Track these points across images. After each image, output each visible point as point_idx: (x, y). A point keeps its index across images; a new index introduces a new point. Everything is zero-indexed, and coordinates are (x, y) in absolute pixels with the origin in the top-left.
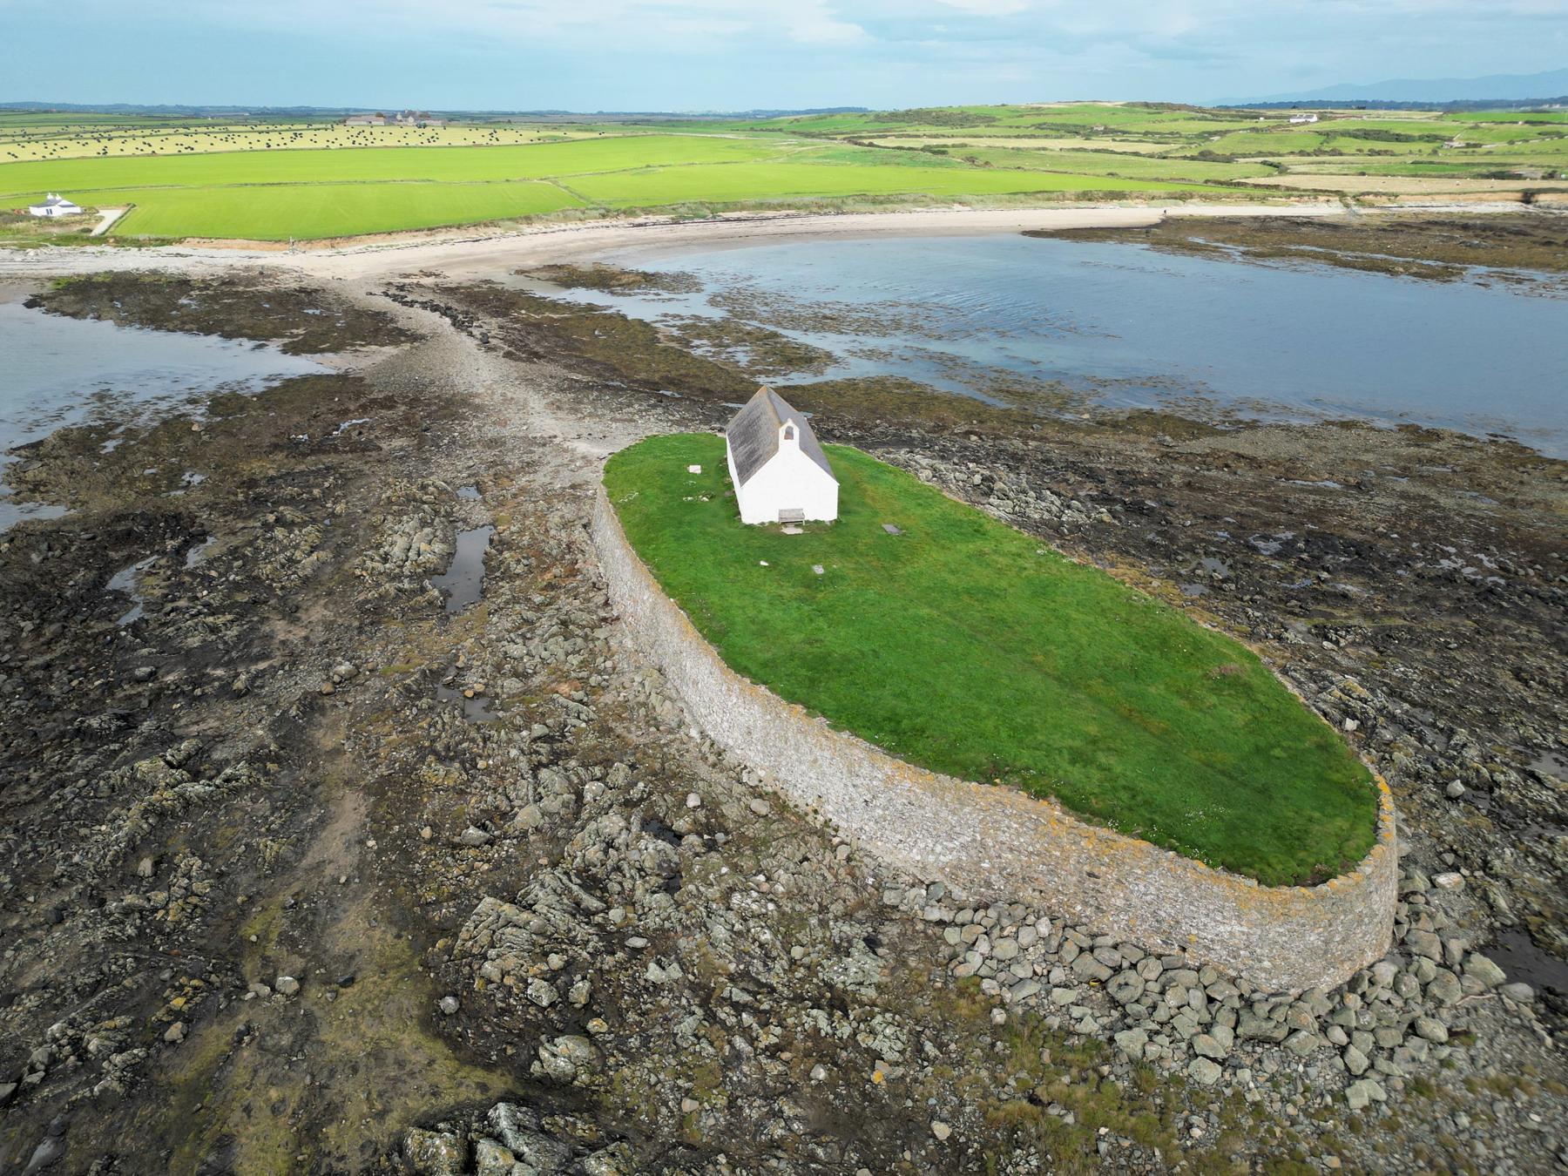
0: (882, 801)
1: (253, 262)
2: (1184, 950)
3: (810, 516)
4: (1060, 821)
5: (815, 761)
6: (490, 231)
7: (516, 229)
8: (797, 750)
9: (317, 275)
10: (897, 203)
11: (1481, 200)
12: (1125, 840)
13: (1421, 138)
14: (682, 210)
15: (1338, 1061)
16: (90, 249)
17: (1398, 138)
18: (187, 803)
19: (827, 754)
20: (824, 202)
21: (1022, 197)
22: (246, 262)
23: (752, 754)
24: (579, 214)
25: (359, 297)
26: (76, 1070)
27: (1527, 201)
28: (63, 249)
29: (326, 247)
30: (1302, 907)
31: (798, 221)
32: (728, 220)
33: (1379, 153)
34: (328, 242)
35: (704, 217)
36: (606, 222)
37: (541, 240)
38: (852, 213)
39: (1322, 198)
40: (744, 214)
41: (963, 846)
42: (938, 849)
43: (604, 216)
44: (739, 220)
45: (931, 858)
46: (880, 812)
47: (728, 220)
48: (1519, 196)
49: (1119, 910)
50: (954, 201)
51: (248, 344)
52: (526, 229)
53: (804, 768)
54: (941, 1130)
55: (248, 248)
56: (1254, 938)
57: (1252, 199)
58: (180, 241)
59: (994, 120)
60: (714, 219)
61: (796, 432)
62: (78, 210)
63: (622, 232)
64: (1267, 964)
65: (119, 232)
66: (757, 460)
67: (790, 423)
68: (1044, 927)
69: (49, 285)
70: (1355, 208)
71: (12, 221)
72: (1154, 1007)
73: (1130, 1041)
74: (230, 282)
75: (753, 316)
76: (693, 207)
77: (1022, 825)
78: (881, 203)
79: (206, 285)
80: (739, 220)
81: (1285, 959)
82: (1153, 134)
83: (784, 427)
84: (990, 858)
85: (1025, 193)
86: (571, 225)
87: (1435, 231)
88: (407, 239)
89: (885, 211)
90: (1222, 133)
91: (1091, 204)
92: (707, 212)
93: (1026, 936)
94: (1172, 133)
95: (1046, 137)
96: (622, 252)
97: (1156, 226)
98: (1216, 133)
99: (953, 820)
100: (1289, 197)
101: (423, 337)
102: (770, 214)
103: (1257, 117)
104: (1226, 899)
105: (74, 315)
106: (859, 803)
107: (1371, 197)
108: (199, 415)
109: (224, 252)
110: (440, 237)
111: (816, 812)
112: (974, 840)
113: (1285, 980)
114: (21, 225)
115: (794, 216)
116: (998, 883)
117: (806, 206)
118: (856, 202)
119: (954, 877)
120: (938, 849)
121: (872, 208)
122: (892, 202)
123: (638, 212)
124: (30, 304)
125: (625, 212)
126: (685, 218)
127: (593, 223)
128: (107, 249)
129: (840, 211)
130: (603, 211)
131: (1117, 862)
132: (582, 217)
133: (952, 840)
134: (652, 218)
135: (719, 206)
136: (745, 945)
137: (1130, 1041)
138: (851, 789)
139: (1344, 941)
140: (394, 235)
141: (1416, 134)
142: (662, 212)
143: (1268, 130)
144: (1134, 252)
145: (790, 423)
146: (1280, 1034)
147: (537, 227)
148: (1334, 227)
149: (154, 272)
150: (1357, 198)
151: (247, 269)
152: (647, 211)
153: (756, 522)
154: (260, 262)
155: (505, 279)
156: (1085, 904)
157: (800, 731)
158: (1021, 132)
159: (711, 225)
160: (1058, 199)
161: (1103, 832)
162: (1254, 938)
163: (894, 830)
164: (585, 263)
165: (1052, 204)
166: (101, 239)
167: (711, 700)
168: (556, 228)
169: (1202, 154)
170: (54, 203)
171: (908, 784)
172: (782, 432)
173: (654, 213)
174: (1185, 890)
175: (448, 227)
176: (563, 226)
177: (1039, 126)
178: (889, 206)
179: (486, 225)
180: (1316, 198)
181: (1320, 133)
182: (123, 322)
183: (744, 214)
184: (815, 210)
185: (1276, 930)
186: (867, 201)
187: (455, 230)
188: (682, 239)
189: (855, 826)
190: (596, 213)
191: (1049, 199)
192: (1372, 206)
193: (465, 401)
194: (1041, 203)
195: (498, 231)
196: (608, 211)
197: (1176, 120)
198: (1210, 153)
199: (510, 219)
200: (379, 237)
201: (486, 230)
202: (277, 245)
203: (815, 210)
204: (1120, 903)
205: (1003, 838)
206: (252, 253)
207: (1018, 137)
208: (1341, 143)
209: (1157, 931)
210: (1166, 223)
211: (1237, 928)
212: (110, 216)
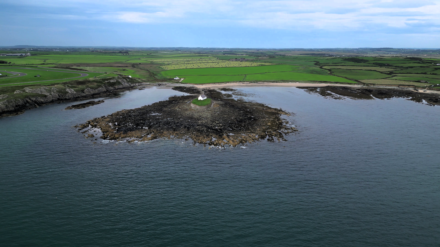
6: (222, 84)
9: (198, 88)
16: (179, 84)
20: (275, 81)
21: (309, 81)
22: (192, 86)
24: (236, 82)
25: (200, 90)
28: (176, 84)
38: (279, 83)
43: (240, 82)
50: (297, 82)
51: (187, 93)
52: (227, 83)
58: (187, 83)
62: (179, 79)
63: (240, 84)
65: (182, 82)
69: (174, 87)
71: (172, 80)
74: (189, 88)
78: (285, 81)
79: (187, 88)
85: (311, 81)
86: (234, 83)
102: (265, 82)
103: (432, 63)
105: (175, 90)
108: (181, 97)
109: (191, 85)
114: (173, 80)
118: (281, 81)
124: (172, 89)
127: (238, 83)
128: (180, 84)
129: (277, 82)
132: (236, 82)
134: (247, 82)
149: (184, 87)
151: (192, 87)
152: (246, 81)
154: (194, 86)
155: (216, 89)
164: (228, 88)
165: (313, 83)
166: (180, 83)
170: (177, 78)
173: (247, 82)
175: (217, 83)
176: (233, 83)
179: (222, 83)
182: (179, 91)
183: (262, 82)
190: (238, 81)
191: (314, 82)
194: (312, 83)
195: (223, 83)
197: (410, 63)
212: (182, 79)
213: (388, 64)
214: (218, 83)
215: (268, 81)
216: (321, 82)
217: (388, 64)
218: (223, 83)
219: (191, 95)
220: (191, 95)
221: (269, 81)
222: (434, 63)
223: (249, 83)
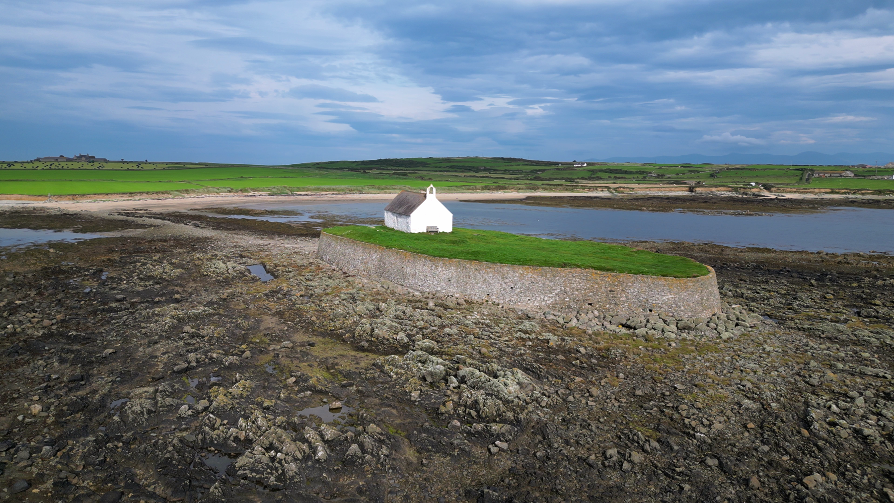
0: (519, 285)
1: (25, 205)
2: (651, 311)
3: (440, 230)
4: (596, 274)
5: (485, 280)
6: (166, 196)
7: (181, 196)
8: (475, 279)
10: (391, 189)
11: (671, 191)
12: (621, 274)
13: (637, 172)
14: (274, 190)
15: (716, 331)
17: (626, 172)
18: (189, 317)
19: (491, 275)
21: (455, 188)
22: (21, 206)
23: (451, 290)
24: (215, 190)
25: (106, 215)
26: (209, 364)
27: (692, 191)
29: (69, 199)
30: (691, 284)
31: (340, 196)
32: (301, 195)
33: (619, 178)
34: (71, 197)
35: (287, 194)
36: (232, 194)
37: (196, 200)
39: (599, 189)
40: (309, 193)
41: (556, 294)
42: (546, 298)
43: (230, 192)
44: (306, 195)
45: (543, 303)
46: (519, 290)
47: (301, 195)
48: (687, 189)
49: (624, 302)
53: (479, 285)
54: (582, 350)
55: (21, 199)
56: (677, 299)
57: (567, 190)
59: (428, 164)
60: (293, 194)
61: (434, 190)
63: (242, 198)
64: (682, 308)
66: (414, 206)
67: (432, 186)
68: (596, 313)
70: (616, 194)
72: (646, 325)
73: (641, 331)
75: (338, 221)
76: (280, 189)
77: (580, 279)
78: (383, 189)
80: (306, 195)
81: (689, 305)
82: (509, 171)
83: (429, 187)
84: (568, 296)
87: (655, 200)
88: (118, 197)
89: (385, 193)
90: (543, 171)
91: (489, 191)
92: (288, 191)
93: (590, 315)
94: (518, 170)
95: (455, 171)
96: (246, 204)
97: (524, 199)
98: (539, 170)
99: (551, 284)
100: (584, 189)
101: (158, 226)
104: (664, 286)
106: (509, 289)
107: (622, 189)
110: (137, 198)
111: (487, 301)
112: (561, 290)
113: (690, 314)
115: (337, 194)
116: (573, 305)
117: (343, 190)
119: (554, 308)
120: (546, 298)
121: (378, 191)
122: (388, 189)
123: (249, 190)
125: (241, 190)
126: (276, 194)
127: (224, 194)
129: (361, 192)
130: (229, 189)
131: (621, 283)
132: (218, 191)
133: (551, 293)
134: (257, 193)
135: (295, 189)
136: (481, 326)
137: (641, 331)
138: (504, 285)
139: (707, 300)
140: (110, 196)
141: (634, 171)
142: (263, 191)
143: (564, 169)
144: (517, 206)
145: (432, 186)
146: (693, 325)
147: (192, 195)
148: (609, 199)
150: (615, 189)
151: (23, 208)
153: (416, 232)
156: (610, 304)
157: (476, 270)
158: (443, 169)
159: (292, 196)
160: (473, 189)
161: (613, 274)
162: (677, 299)
163: (526, 296)
167: (426, 276)
168: (203, 196)
169: (535, 178)
171: (530, 275)
172: (428, 190)
173: (258, 191)
174: (649, 287)
176: (207, 195)
177: (451, 167)
178: (387, 191)
179: (163, 193)
180: (596, 189)
181: (589, 171)
183: (309, 193)
184: (348, 191)
185: (684, 295)
186: (375, 188)
187: (145, 194)
188: (278, 201)
189: (507, 300)
190: (226, 190)
191: (468, 189)
192: (623, 193)
193: (207, 238)
194: (465, 191)
195: (170, 196)
196: (232, 189)
197: (519, 165)
198: (539, 177)
199: (177, 191)
200: (101, 196)
201: (163, 195)
202: (40, 198)
203: (348, 191)
204: (624, 299)
205: (574, 286)
206: (24, 202)
207: (441, 171)
208: (599, 174)
209: (640, 306)
210: (528, 198)
211: (670, 296)
213: (485, 168)
214: (148, 193)
215: (329, 190)
216: (489, 190)
217: (485, 168)
218: (167, 192)
219: (89, 236)
220: (89, 236)
221: (333, 190)
222: (562, 165)
223: (270, 195)
